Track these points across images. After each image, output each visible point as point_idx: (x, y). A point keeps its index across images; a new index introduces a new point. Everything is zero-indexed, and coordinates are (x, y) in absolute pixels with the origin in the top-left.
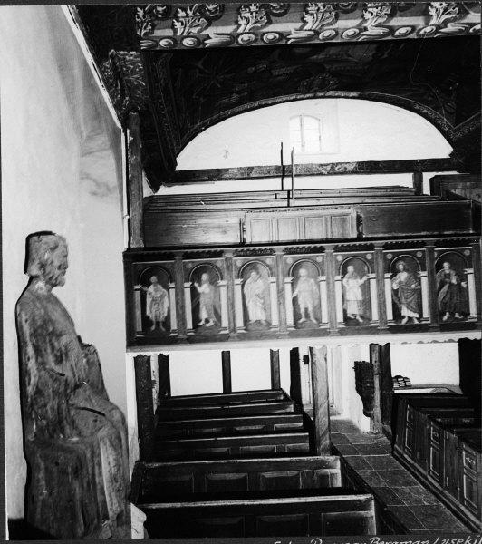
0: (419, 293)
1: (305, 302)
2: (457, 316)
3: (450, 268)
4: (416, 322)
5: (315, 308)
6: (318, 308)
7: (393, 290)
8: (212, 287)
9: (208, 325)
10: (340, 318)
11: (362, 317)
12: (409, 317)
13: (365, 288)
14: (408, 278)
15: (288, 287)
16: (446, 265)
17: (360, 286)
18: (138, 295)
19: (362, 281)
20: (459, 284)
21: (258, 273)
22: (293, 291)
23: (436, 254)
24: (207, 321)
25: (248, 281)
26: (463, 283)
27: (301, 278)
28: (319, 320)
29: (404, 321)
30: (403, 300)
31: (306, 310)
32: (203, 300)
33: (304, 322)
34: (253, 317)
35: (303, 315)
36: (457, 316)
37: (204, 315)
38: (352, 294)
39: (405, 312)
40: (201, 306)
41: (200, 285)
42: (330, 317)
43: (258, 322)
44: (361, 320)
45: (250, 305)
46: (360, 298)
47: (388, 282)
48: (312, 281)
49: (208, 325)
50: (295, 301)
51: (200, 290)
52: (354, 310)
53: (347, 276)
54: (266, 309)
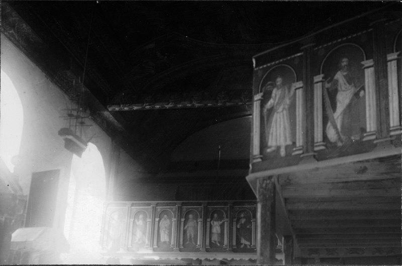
7: (237, 228)
11: (219, 243)
12: (245, 244)
13: (222, 226)
14: (245, 223)
19: (221, 222)
22: (184, 226)
25: (163, 219)
27: (190, 220)
29: (242, 246)
31: (191, 237)
35: (188, 240)
39: (243, 241)
41: (138, 221)
44: (218, 245)
46: (219, 232)
47: (235, 223)
48: (195, 221)
50: (185, 232)
51: (138, 223)
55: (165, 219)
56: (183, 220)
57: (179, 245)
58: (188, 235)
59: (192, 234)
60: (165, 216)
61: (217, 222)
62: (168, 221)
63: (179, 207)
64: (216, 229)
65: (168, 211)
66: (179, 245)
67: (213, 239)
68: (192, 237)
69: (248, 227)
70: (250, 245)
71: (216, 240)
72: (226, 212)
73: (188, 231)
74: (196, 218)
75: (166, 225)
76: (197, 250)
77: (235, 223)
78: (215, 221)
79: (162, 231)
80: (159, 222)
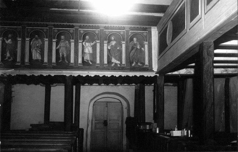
0: (120, 51)
2: (139, 64)
3: (137, 41)
4: (119, 66)
7: (108, 49)
10: (80, 61)
11: (91, 62)
12: (115, 63)
13: (94, 47)
14: (116, 44)
15: (54, 44)
16: (135, 39)
17: (92, 46)
20: (141, 49)
22: (57, 46)
23: (130, 34)
24: (9, 58)
26: (142, 48)
28: (69, 61)
29: (113, 65)
30: (113, 55)
33: (61, 62)
34: (34, 57)
36: (139, 64)
38: (87, 49)
39: (114, 60)
42: (75, 60)
44: (91, 63)
46: (91, 52)
48: (67, 42)
52: (87, 57)
53: (85, 40)
58: (61, 54)
62: (39, 40)
67: (85, 58)
68: (65, 56)
71: (89, 59)
73: (60, 51)
75: (38, 45)
78: (87, 42)
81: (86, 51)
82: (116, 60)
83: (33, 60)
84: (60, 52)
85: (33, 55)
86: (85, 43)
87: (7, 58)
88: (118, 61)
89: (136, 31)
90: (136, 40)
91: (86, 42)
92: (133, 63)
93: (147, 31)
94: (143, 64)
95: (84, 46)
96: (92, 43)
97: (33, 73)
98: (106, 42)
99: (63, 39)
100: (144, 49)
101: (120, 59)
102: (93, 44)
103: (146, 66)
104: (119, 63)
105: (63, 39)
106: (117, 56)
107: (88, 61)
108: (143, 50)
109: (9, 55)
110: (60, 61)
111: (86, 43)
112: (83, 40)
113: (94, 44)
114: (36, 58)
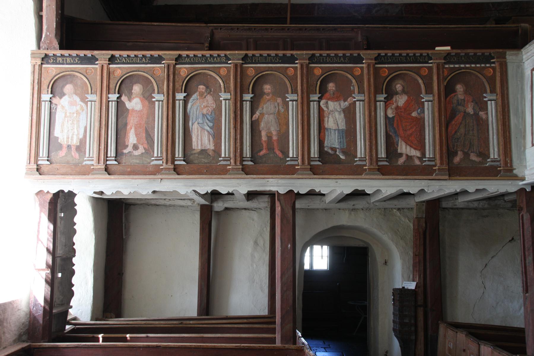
0: (420, 122)
1: (269, 126)
2: (473, 157)
3: (466, 92)
4: (417, 162)
5: (279, 132)
6: (284, 137)
7: (386, 117)
8: (147, 103)
9: (136, 153)
11: (344, 152)
12: (407, 155)
13: (349, 114)
16: (460, 88)
17: (344, 111)
18: (45, 107)
19: (347, 103)
20: (476, 115)
21: (207, 87)
22: (252, 113)
24: (135, 147)
25: (195, 96)
26: (481, 113)
28: (286, 153)
29: (401, 161)
31: (270, 137)
32: (132, 121)
33: (264, 155)
35: (265, 145)
36: (473, 157)
37: (132, 138)
38: (331, 119)
39: (403, 148)
40: (128, 127)
41: (130, 100)
43: (203, 152)
44: (342, 157)
45: (195, 129)
46: (342, 125)
47: (381, 106)
48: (279, 100)
49: (136, 153)
50: (254, 125)
51: (129, 105)
52: (333, 141)
53: (327, 95)
54: (217, 137)
55: (201, 95)
56: (248, 97)
57: (242, 160)
58: (263, 134)
59: (274, 133)
60: (202, 88)
61: (336, 103)
62: (209, 98)
63: (236, 65)
64: (335, 121)
65: (204, 74)
66: (242, 161)
68: (275, 138)
69: (414, 114)
70: (420, 159)
71: (336, 145)
72: (359, 80)
73: (262, 125)
74: (281, 93)
75: (205, 111)
76: (289, 171)
77: (381, 106)
78: (332, 99)
79: (196, 126)
80: (186, 101)
81: (329, 123)
82: (408, 147)
83: (194, 152)
84: (261, 129)
85: (194, 139)
86: (327, 103)
87: (129, 149)
88: (415, 149)
89: (462, 66)
90: (462, 90)
91: (329, 99)
92: (456, 154)
93: (494, 63)
94: (485, 155)
95: (323, 110)
96: (345, 100)
97: (194, 186)
98: (383, 99)
99: (268, 94)
100: (487, 114)
101: (421, 147)
102: (347, 103)
103: (493, 163)
104: (418, 154)
105: (268, 94)
106: (411, 134)
107: (336, 151)
108: (484, 117)
109: (136, 139)
110: (262, 153)
111: (329, 102)
112: (320, 95)
113: (350, 104)
114: (202, 145)
